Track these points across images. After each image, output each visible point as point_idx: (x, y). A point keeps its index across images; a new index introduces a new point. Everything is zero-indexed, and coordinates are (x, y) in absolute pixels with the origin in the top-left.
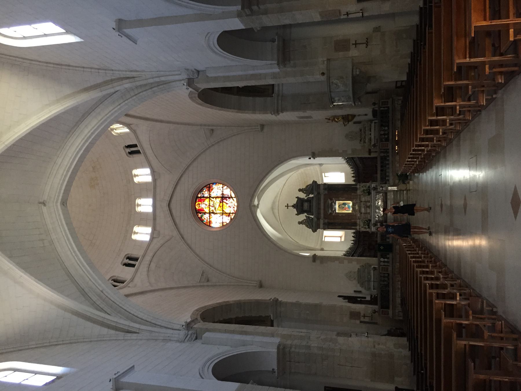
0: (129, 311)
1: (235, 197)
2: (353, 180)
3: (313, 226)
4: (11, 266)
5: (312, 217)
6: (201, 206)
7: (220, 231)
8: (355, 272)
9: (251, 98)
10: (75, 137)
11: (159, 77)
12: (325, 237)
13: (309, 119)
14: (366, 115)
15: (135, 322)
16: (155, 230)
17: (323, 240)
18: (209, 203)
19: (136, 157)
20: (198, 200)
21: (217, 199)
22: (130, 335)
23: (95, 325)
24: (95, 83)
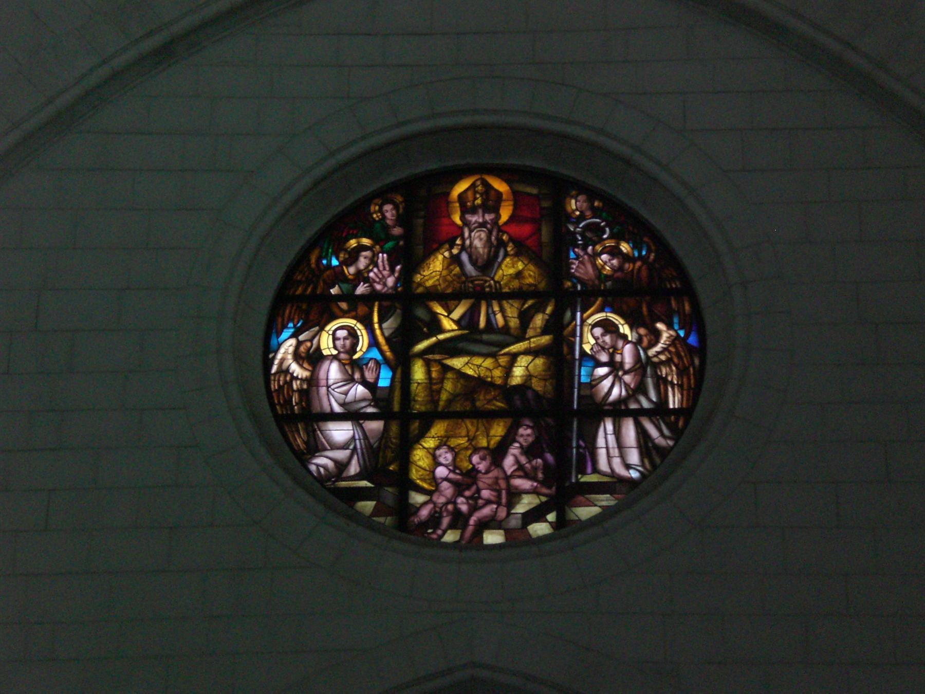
1: (558, 525)
6: (473, 219)
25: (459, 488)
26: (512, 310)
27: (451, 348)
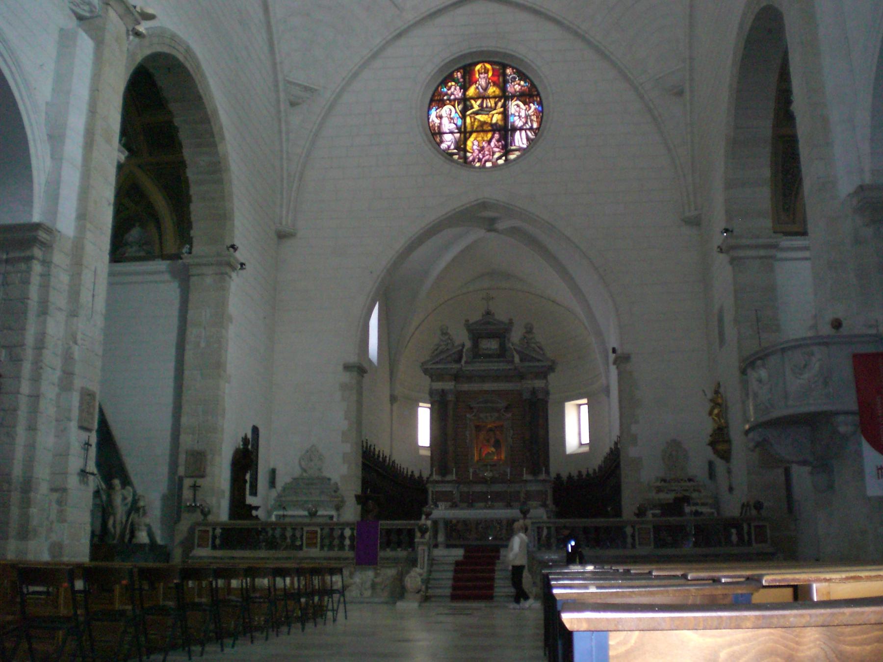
1: (506, 160)
3: (437, 363)
6: (482, 76)
8: (320, 470)
9: (767, 173)
14: (731, 489)
17: (421, 404)
25: (480, 152)
27: (477, 113)
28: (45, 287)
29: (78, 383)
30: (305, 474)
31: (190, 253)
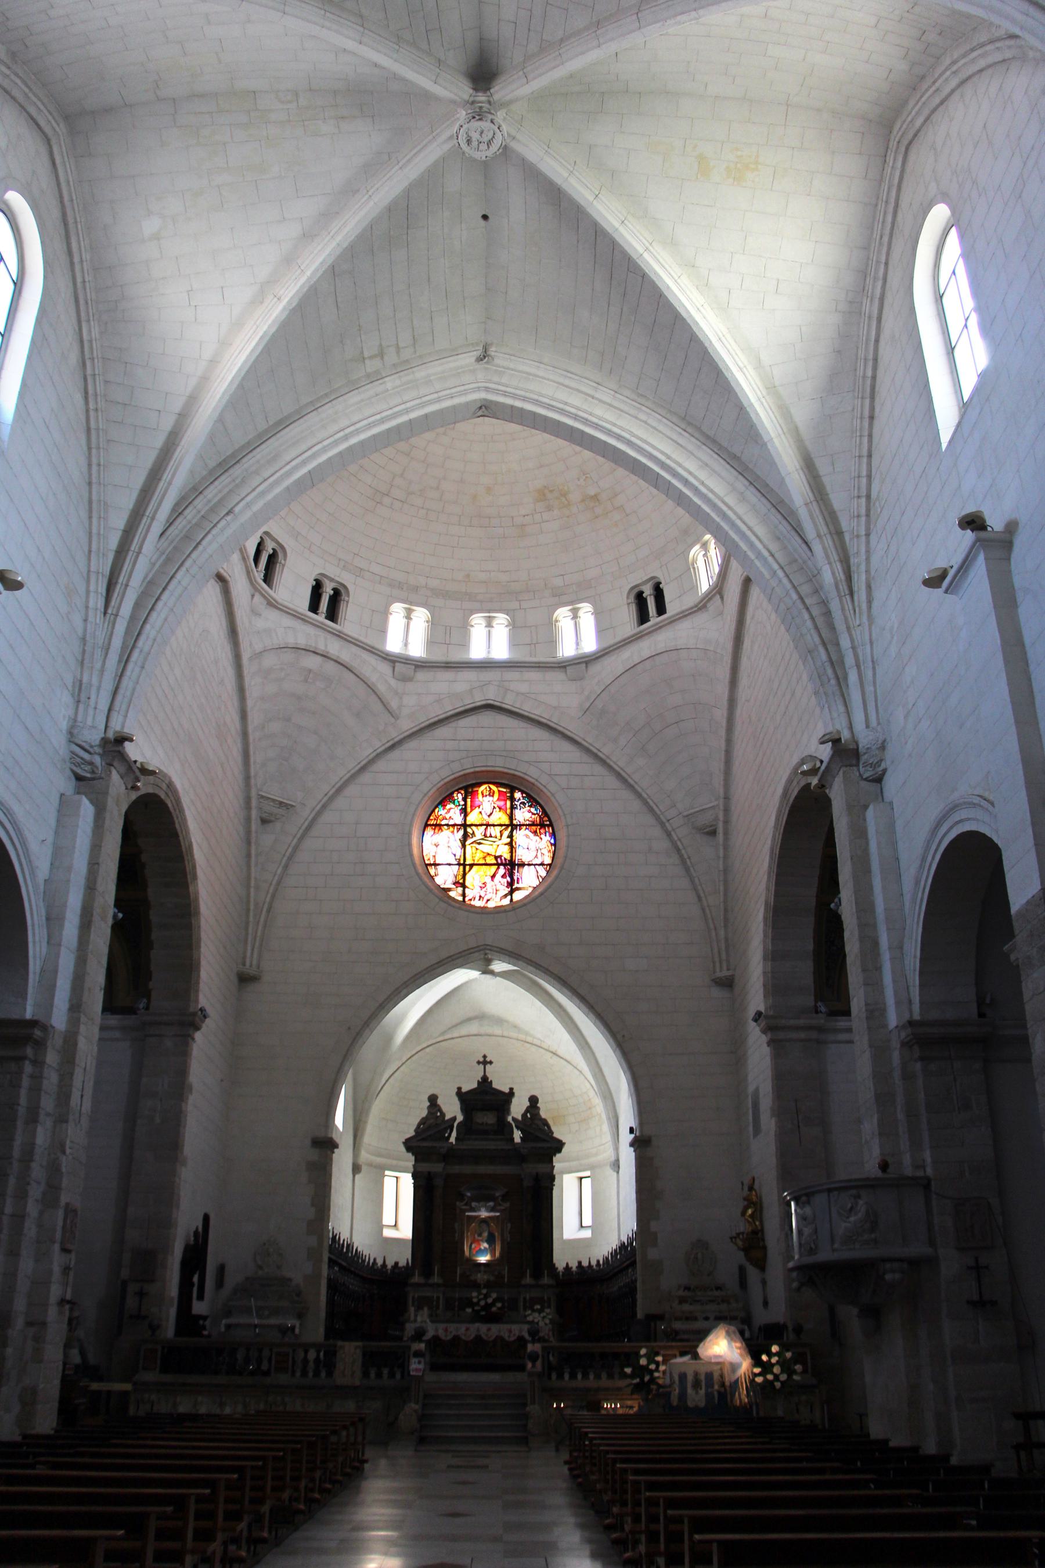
0: (171, 587)
1: (511, 900)
2: (570, 1266)
3: (424, 1139)
4: (308, 273)
5: (452, 1140)
7: (411, 855)
8: (279, 1267)
9: (810, 947)
10: (675, 437)
11: (858, 666)
12: (397, 1178)
13: (751, 1128)
14: (766, 1304)
15: (137, 605)
16: (417, 666)
17: (387, 1173)
18: (494, 825)
19: (627, 614)
20: (505, 790)
21: (507, 848)
22: (102, 589)
23: (135, 495)
24: (828, 488)
26: (499, 829)
28: (36, 1090)
29: (64, 1199)
30: (260, 1272)
31: (147, 1008)
